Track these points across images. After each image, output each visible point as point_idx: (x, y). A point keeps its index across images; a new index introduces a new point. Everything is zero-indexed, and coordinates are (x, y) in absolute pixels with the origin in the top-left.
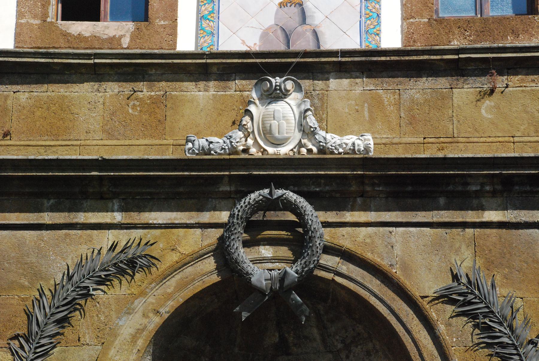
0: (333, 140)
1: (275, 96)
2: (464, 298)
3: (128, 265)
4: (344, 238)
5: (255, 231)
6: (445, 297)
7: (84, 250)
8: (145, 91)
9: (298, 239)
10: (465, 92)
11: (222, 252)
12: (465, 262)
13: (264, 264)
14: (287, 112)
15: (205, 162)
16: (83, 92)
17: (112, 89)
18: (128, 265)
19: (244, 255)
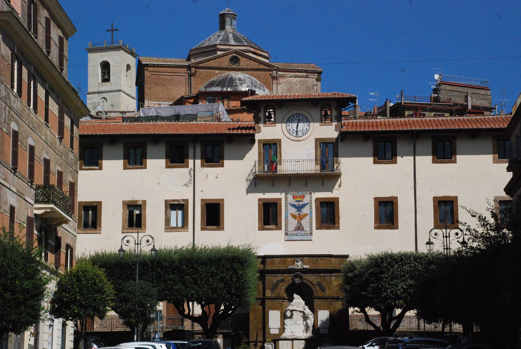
0: (305, 266)
1: (298, 262)
2: (319, 284)
3: (282, 281)
4: (306, 278)
5: (296, 276)
6: (317, 284)
7: (277, 279)
8: (283, 259)
9: (301, 278)
10: (319, 259)
11: (293, 279)
12: (319, 280)
13: (297, 280)
14: (299, 263)
15: (290, 269)
16: (276, 259)
17: (279, 259)
18: (282, 281)
19: (295, 279)
